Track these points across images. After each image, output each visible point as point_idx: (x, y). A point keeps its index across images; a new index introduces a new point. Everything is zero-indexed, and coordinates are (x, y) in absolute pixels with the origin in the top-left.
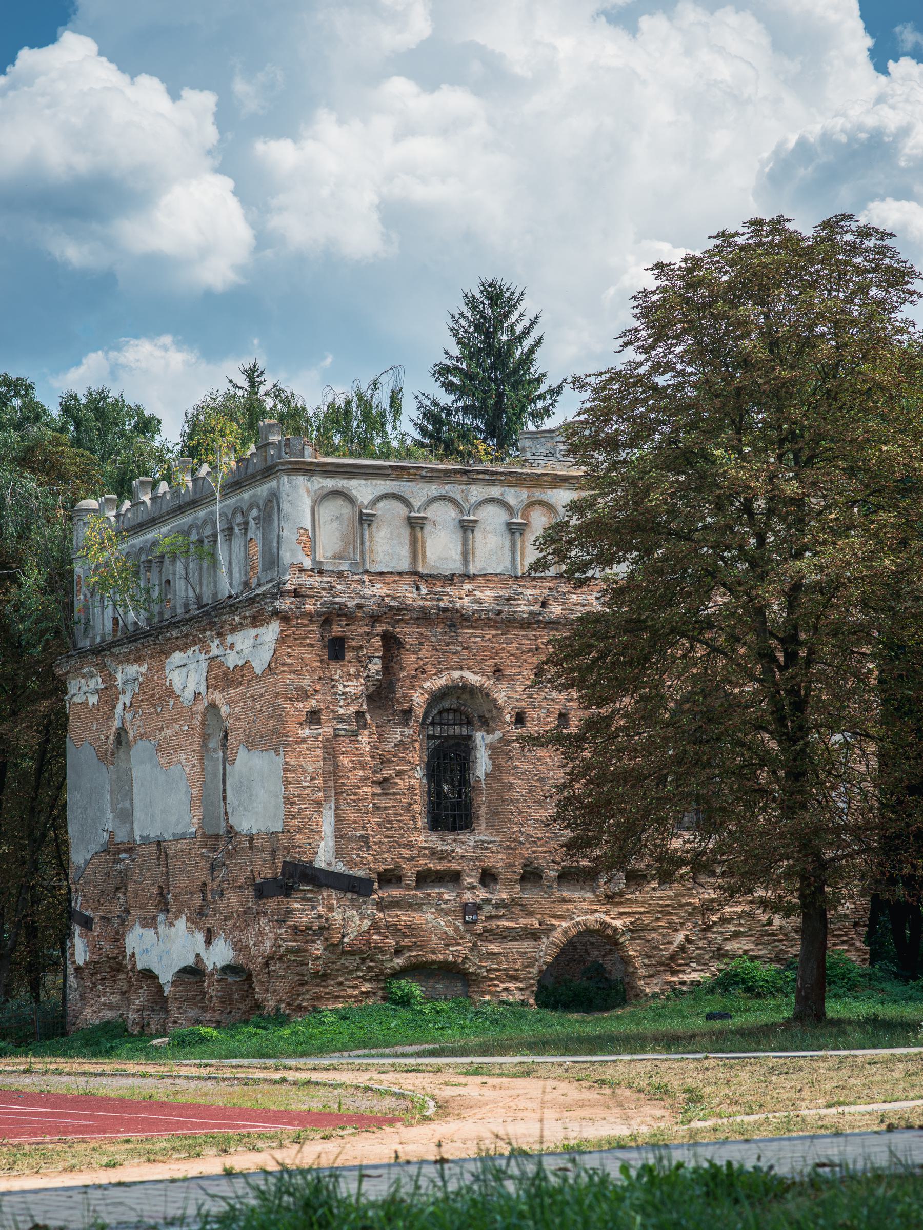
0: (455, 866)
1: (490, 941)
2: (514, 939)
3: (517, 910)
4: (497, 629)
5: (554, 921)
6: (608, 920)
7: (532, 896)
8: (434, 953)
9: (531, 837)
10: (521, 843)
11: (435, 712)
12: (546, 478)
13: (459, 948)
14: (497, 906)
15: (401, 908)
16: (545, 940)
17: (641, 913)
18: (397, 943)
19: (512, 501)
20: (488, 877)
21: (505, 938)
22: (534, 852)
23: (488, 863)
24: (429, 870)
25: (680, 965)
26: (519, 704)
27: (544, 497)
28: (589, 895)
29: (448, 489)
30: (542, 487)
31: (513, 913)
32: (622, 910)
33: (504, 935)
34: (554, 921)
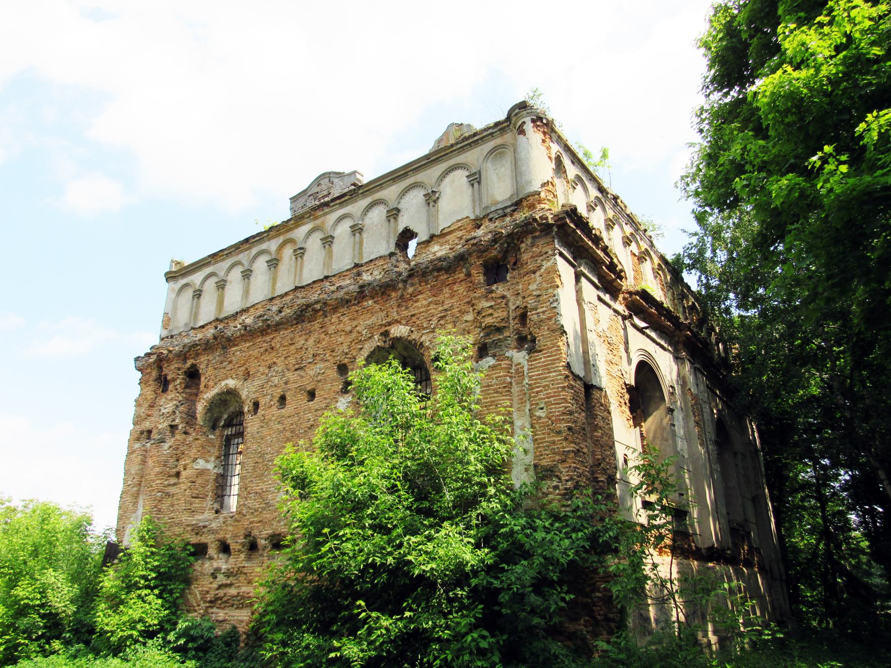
4: (249, 341)
9: (251, 509)
11: (225, 416)
12: (292, 222)
14: (228, 574)
22: (251, 523)
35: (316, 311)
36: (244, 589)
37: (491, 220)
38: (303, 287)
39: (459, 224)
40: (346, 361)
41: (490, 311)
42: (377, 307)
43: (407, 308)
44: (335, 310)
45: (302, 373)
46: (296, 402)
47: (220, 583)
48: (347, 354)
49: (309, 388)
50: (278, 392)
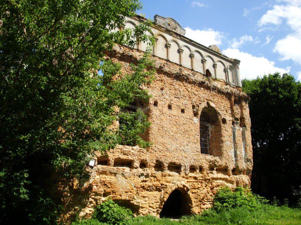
0: (130, 158)
1: (142, 191)
2: (151, 191)
3: (152, 178)
5: (167, 184)
6: (185, 184)
7: (159, 174)
8: (121, 196)
10: (156, 151)
13: (131, 193)
15: (106, 175)
16: (163, 191)
17: (194, 182)
18: (105, 191)
19: (154, 33)
20: (143, 165)
21: (147, 190)
23: (143, 158)
24: (120, 158)
25: (205, 202)
26: (156, 98)
27: (163, 35)
28: (177, 174)
29: (133, 21)
30: (161, 31)
31: (151, 180)
32: (188, 180)
33: (149, 189)
34: (167, 184)
35: (184, 78)
36: (154, 183)
37: (230, 86)
38: (170, 62)
39: (222, 80)
40: (195, 105)
41: (237, 114)
42: (204, 92)
43: (214, 98)
44: (190, 83)
45: (178, 100)
46: (175, 111)
47: (142, 180)
48: (195, 102)
49: (182, 108)
50: (168, 103)
